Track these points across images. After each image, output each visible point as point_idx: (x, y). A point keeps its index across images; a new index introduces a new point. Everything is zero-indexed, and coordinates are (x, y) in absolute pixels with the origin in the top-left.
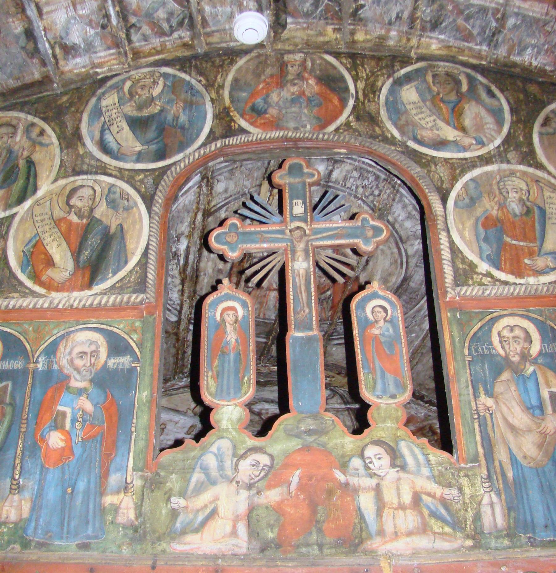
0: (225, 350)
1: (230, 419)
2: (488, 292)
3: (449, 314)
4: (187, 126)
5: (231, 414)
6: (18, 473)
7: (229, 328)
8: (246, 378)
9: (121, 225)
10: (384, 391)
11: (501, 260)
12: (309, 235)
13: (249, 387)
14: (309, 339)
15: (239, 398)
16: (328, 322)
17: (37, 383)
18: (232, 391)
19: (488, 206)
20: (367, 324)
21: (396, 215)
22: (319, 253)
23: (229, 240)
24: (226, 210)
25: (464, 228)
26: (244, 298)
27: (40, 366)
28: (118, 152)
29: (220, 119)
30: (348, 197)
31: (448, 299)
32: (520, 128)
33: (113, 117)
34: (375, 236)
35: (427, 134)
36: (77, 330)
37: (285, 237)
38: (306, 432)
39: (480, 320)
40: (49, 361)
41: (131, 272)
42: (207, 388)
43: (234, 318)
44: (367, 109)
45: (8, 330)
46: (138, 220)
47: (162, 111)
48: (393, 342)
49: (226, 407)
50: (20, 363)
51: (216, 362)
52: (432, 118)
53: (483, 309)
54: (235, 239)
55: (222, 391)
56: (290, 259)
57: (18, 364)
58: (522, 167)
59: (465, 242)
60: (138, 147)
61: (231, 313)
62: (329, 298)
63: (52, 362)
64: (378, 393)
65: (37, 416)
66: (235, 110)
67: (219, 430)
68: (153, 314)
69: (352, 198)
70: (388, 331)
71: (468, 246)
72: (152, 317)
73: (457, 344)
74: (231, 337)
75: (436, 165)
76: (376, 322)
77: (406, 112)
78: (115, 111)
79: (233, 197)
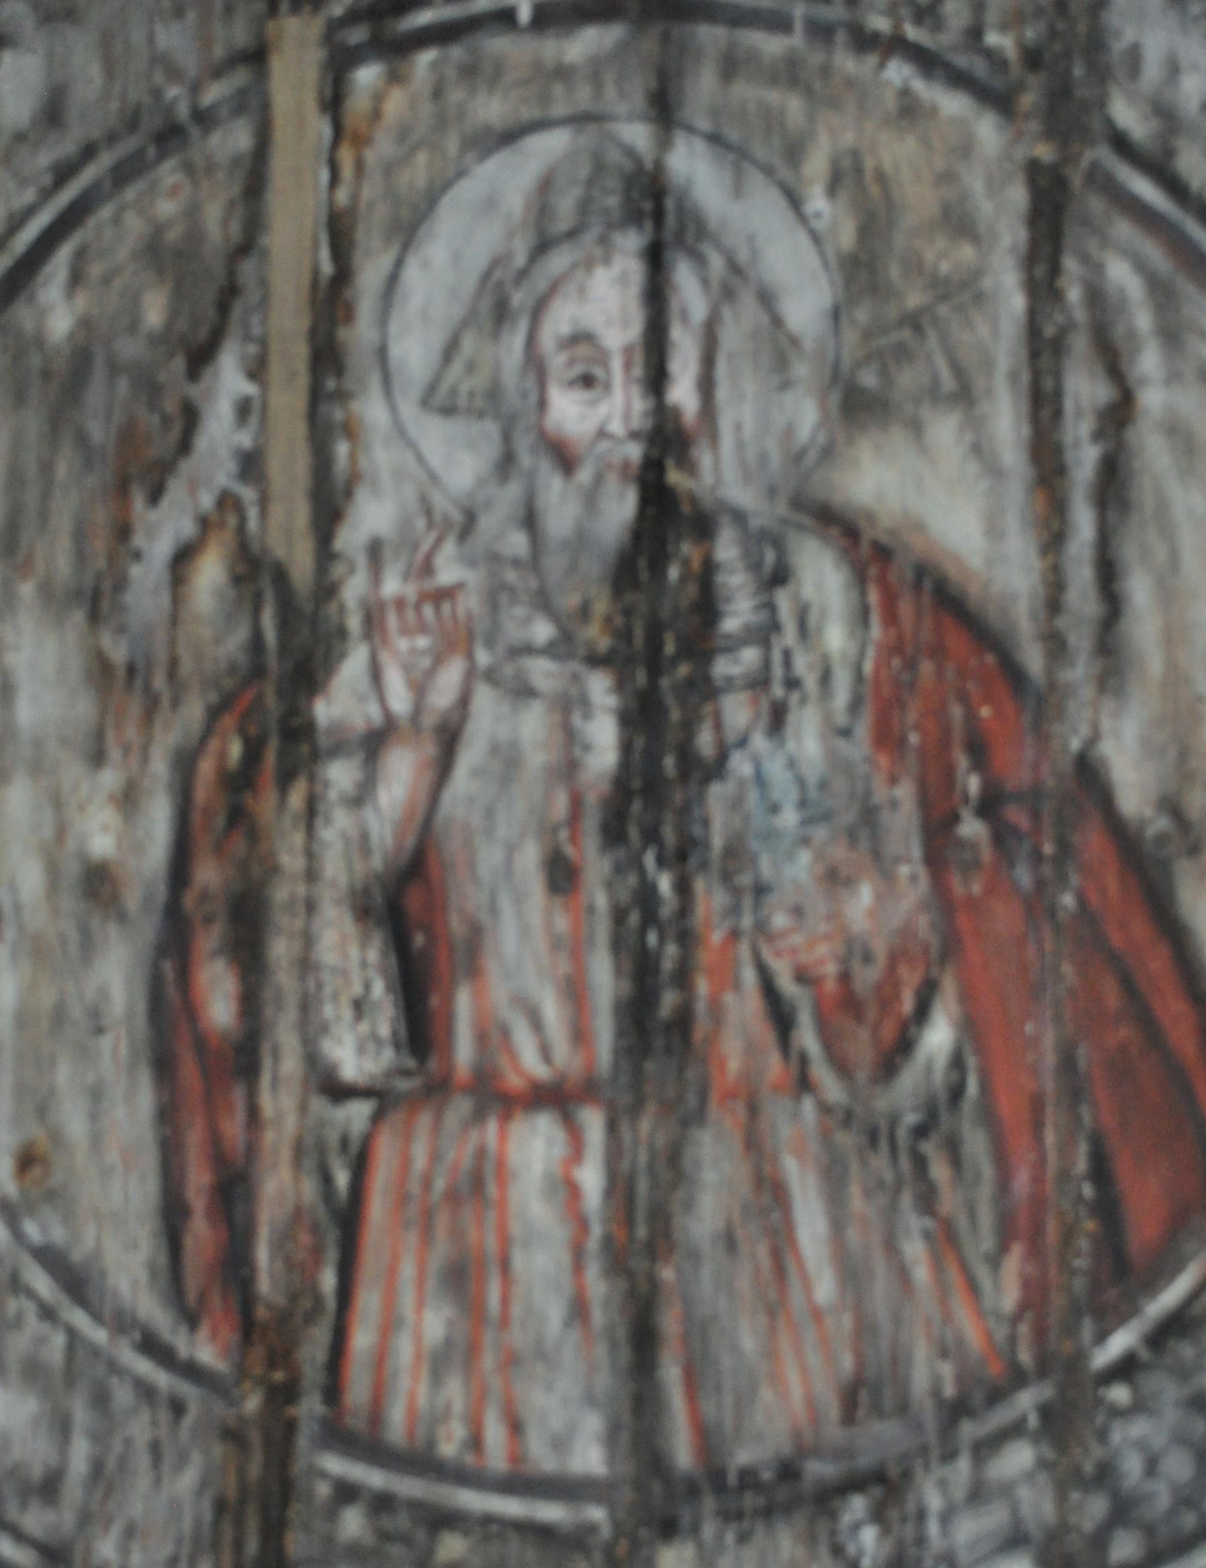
16: (1026, 1401)
21: (1152, 70)
24: (76, 279)
30: (816, 58)
69: (847, 63)
79: (105, 160)
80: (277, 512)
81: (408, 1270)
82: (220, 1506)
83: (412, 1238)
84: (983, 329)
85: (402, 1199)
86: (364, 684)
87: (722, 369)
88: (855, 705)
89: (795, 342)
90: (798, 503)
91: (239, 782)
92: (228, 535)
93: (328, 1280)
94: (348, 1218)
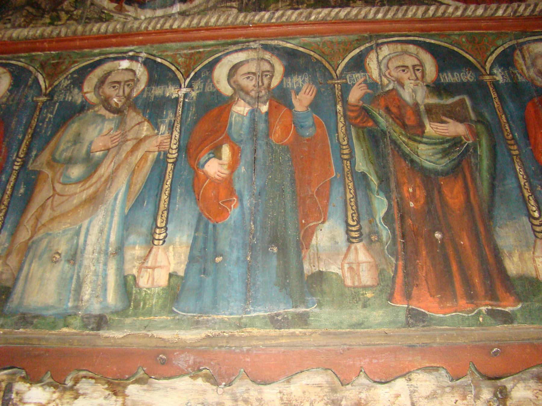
6: (534, 209)
17: (506, 97)
27: (499, 78)
36: (529, 42)
40: (509, 73)
45: (433, 41)
50: (469, 76)
57: (468, 77)
63: (514, 74)
65: (527, 135)
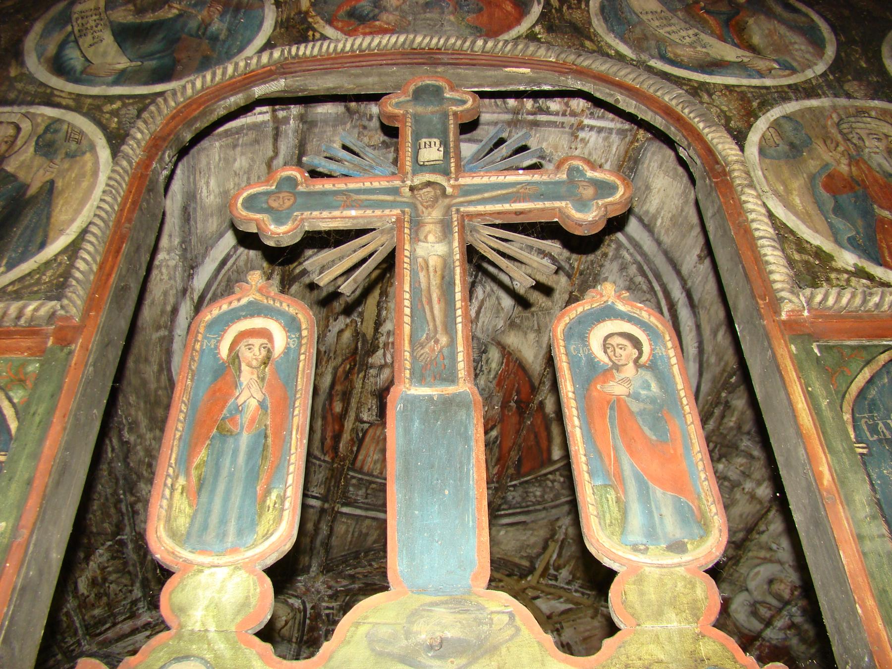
0: (229, 425)
1: (215, 606)
2: (876, 299)
3: (793, 348)
4: (222, 37)
5: (220, 591)
7: (247, 375)
8: (274, 496)
9: (52, 182)
10: (651, 533)
11: (881, 248)
12: (452, 196)
13: (279, 519)
14: (448, 404)
15: (249, 548)
18: (232, 528)
19: (827, 157)
20: (592, 373)
22: (473, 230)
23: (274, 204)
25: (788, 191)
26: (292, 311)
28: (82, 72)
29: (287, 28)
31: (784, 316)
32: (856, 51)
33: (88, 26)
34: (597, 196)
35: (685, 53)
37: (399, 199)
38: (431, 647)
39: (868, 363)
41: (47, 264)
42: (168, 520)
43: (264, 352)
44: (567, 17)
46: (89, 173)
47: (180, 16)
48: (660, 413)
49: (207, 571)
51: (202, 454)
52: (691, 32)
53: (870, 337)
54: (288, 204)
55: (205, 527)
56: (407, 237)
58: (876, 103)
59: (796, 214)
60: (123, 63)
61: (257, 342)
62: (494, 442)
64: (636, 535)
66: (318, 14)
67: (179, 637)
68: (69, 344)
70: (648, 387)
71: (804, 222)
72: (66, 350)
73: (828, 414)
74: (250, 394)
75: (710, 95)
76: (617, 367)
77: (641, 22)
78: (95, 17)
80: (365, 324)
81: (372, 448)
82: (327, 478)
83: (374, 445)
84: (548, 319)
85: (373, 438)
86: (381, 356)
87: (483, 310)
88: (495, 377)
89: (502, 309)
90: (492, 340)
91: (348, 374)
92: (353, 328)
93: (355, 449)
94: (361, 441)
